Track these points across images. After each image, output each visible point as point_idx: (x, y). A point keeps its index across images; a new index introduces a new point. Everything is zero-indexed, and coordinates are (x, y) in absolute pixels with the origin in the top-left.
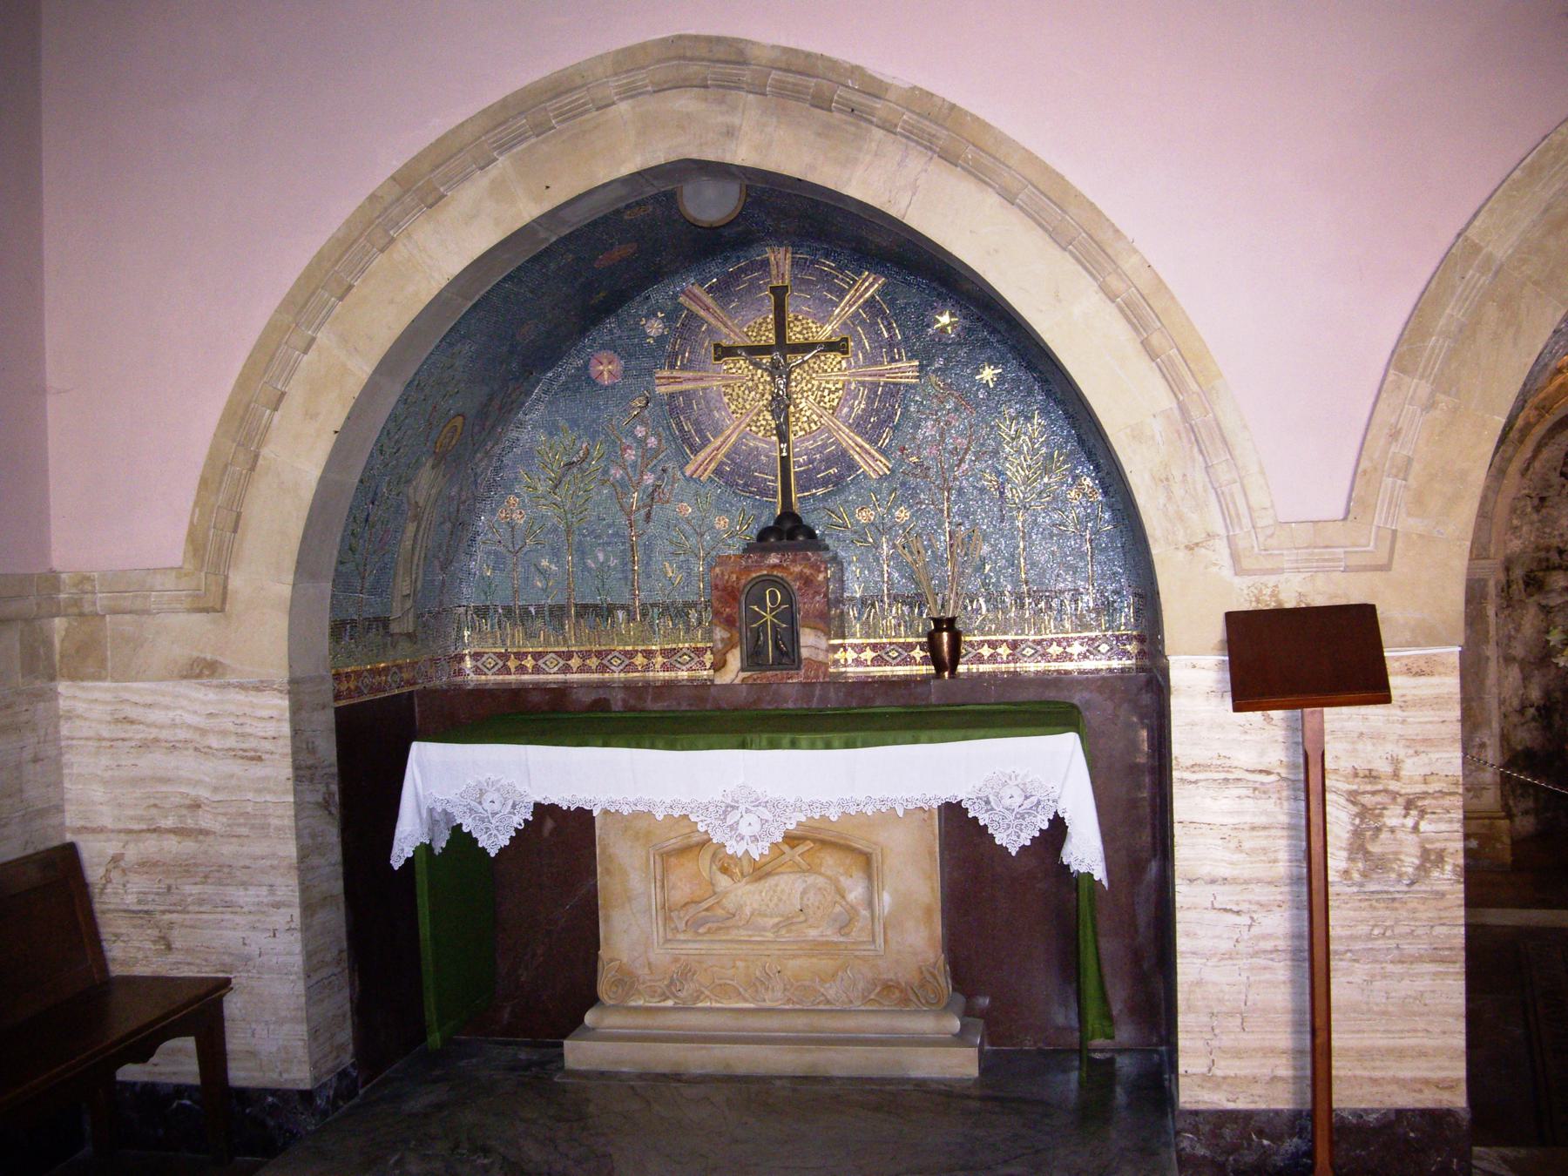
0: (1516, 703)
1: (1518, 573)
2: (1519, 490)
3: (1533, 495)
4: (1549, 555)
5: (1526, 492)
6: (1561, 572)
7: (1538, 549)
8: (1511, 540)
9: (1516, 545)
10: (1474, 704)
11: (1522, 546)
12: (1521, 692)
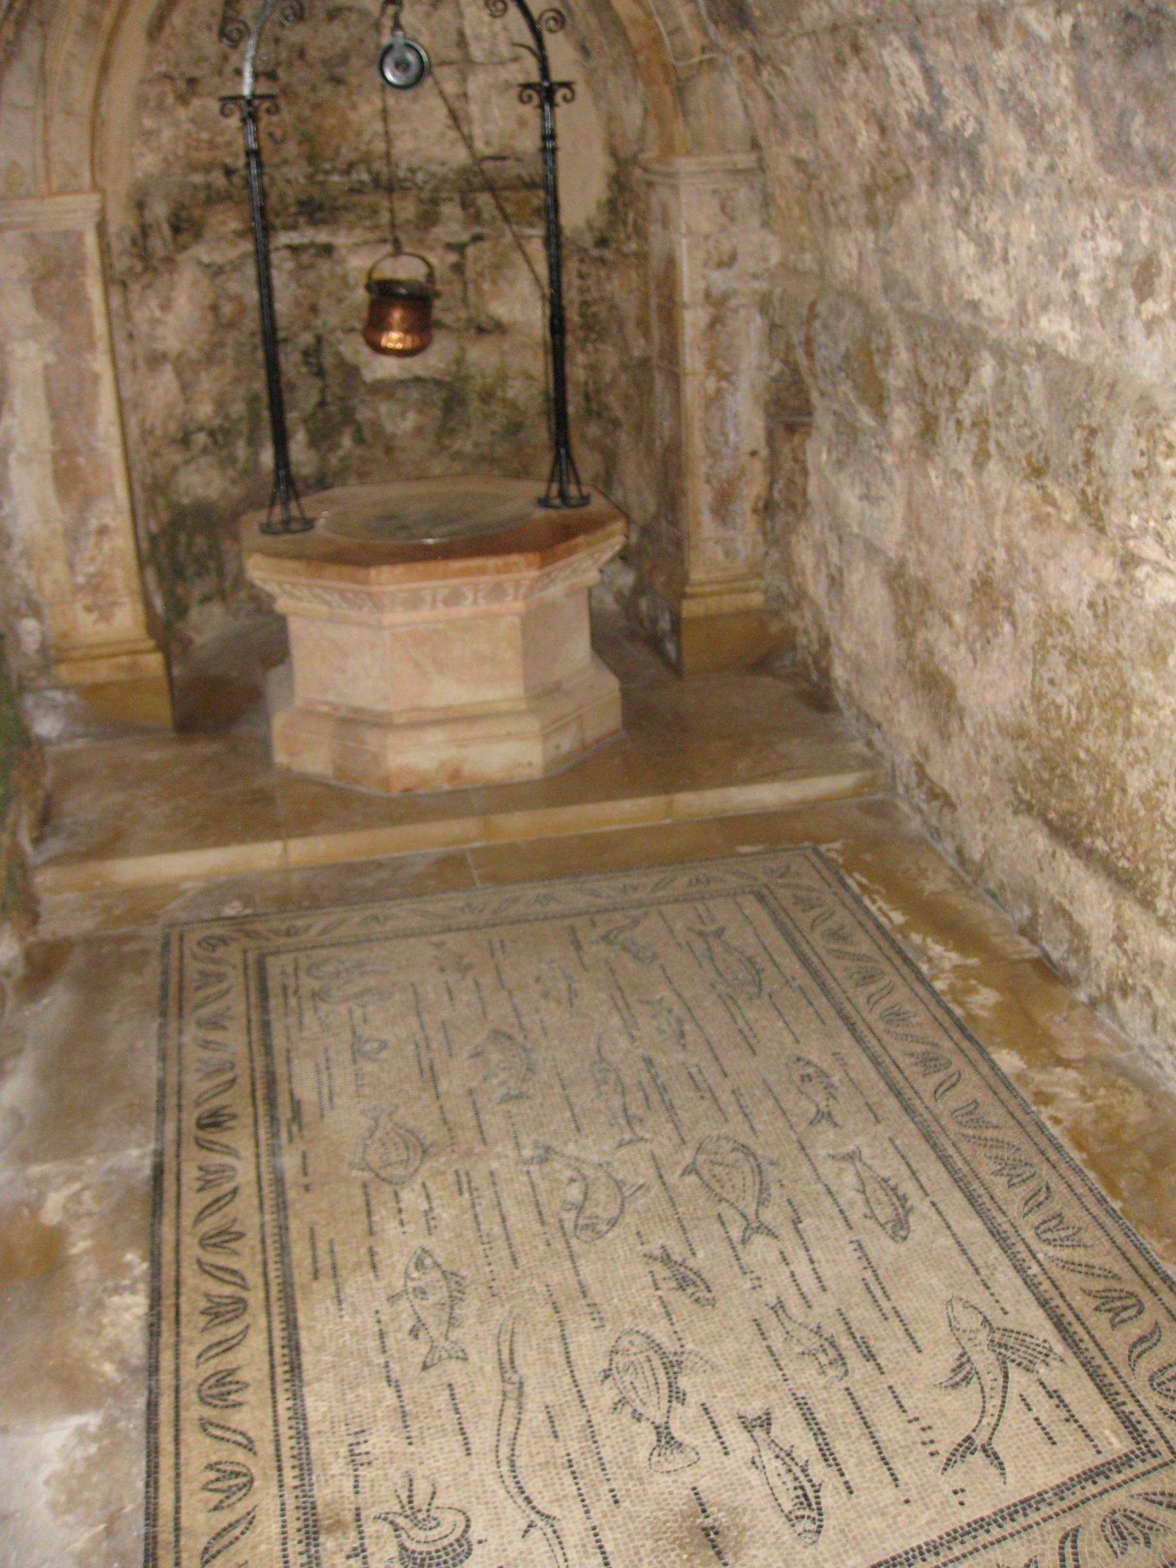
1: (159, 211)
3: (176, 74)
4: (210, 178)
5: (163, 68)
8: (142, 155)
9: (149, 162)
10: (81, 460)
12: (179, 410)
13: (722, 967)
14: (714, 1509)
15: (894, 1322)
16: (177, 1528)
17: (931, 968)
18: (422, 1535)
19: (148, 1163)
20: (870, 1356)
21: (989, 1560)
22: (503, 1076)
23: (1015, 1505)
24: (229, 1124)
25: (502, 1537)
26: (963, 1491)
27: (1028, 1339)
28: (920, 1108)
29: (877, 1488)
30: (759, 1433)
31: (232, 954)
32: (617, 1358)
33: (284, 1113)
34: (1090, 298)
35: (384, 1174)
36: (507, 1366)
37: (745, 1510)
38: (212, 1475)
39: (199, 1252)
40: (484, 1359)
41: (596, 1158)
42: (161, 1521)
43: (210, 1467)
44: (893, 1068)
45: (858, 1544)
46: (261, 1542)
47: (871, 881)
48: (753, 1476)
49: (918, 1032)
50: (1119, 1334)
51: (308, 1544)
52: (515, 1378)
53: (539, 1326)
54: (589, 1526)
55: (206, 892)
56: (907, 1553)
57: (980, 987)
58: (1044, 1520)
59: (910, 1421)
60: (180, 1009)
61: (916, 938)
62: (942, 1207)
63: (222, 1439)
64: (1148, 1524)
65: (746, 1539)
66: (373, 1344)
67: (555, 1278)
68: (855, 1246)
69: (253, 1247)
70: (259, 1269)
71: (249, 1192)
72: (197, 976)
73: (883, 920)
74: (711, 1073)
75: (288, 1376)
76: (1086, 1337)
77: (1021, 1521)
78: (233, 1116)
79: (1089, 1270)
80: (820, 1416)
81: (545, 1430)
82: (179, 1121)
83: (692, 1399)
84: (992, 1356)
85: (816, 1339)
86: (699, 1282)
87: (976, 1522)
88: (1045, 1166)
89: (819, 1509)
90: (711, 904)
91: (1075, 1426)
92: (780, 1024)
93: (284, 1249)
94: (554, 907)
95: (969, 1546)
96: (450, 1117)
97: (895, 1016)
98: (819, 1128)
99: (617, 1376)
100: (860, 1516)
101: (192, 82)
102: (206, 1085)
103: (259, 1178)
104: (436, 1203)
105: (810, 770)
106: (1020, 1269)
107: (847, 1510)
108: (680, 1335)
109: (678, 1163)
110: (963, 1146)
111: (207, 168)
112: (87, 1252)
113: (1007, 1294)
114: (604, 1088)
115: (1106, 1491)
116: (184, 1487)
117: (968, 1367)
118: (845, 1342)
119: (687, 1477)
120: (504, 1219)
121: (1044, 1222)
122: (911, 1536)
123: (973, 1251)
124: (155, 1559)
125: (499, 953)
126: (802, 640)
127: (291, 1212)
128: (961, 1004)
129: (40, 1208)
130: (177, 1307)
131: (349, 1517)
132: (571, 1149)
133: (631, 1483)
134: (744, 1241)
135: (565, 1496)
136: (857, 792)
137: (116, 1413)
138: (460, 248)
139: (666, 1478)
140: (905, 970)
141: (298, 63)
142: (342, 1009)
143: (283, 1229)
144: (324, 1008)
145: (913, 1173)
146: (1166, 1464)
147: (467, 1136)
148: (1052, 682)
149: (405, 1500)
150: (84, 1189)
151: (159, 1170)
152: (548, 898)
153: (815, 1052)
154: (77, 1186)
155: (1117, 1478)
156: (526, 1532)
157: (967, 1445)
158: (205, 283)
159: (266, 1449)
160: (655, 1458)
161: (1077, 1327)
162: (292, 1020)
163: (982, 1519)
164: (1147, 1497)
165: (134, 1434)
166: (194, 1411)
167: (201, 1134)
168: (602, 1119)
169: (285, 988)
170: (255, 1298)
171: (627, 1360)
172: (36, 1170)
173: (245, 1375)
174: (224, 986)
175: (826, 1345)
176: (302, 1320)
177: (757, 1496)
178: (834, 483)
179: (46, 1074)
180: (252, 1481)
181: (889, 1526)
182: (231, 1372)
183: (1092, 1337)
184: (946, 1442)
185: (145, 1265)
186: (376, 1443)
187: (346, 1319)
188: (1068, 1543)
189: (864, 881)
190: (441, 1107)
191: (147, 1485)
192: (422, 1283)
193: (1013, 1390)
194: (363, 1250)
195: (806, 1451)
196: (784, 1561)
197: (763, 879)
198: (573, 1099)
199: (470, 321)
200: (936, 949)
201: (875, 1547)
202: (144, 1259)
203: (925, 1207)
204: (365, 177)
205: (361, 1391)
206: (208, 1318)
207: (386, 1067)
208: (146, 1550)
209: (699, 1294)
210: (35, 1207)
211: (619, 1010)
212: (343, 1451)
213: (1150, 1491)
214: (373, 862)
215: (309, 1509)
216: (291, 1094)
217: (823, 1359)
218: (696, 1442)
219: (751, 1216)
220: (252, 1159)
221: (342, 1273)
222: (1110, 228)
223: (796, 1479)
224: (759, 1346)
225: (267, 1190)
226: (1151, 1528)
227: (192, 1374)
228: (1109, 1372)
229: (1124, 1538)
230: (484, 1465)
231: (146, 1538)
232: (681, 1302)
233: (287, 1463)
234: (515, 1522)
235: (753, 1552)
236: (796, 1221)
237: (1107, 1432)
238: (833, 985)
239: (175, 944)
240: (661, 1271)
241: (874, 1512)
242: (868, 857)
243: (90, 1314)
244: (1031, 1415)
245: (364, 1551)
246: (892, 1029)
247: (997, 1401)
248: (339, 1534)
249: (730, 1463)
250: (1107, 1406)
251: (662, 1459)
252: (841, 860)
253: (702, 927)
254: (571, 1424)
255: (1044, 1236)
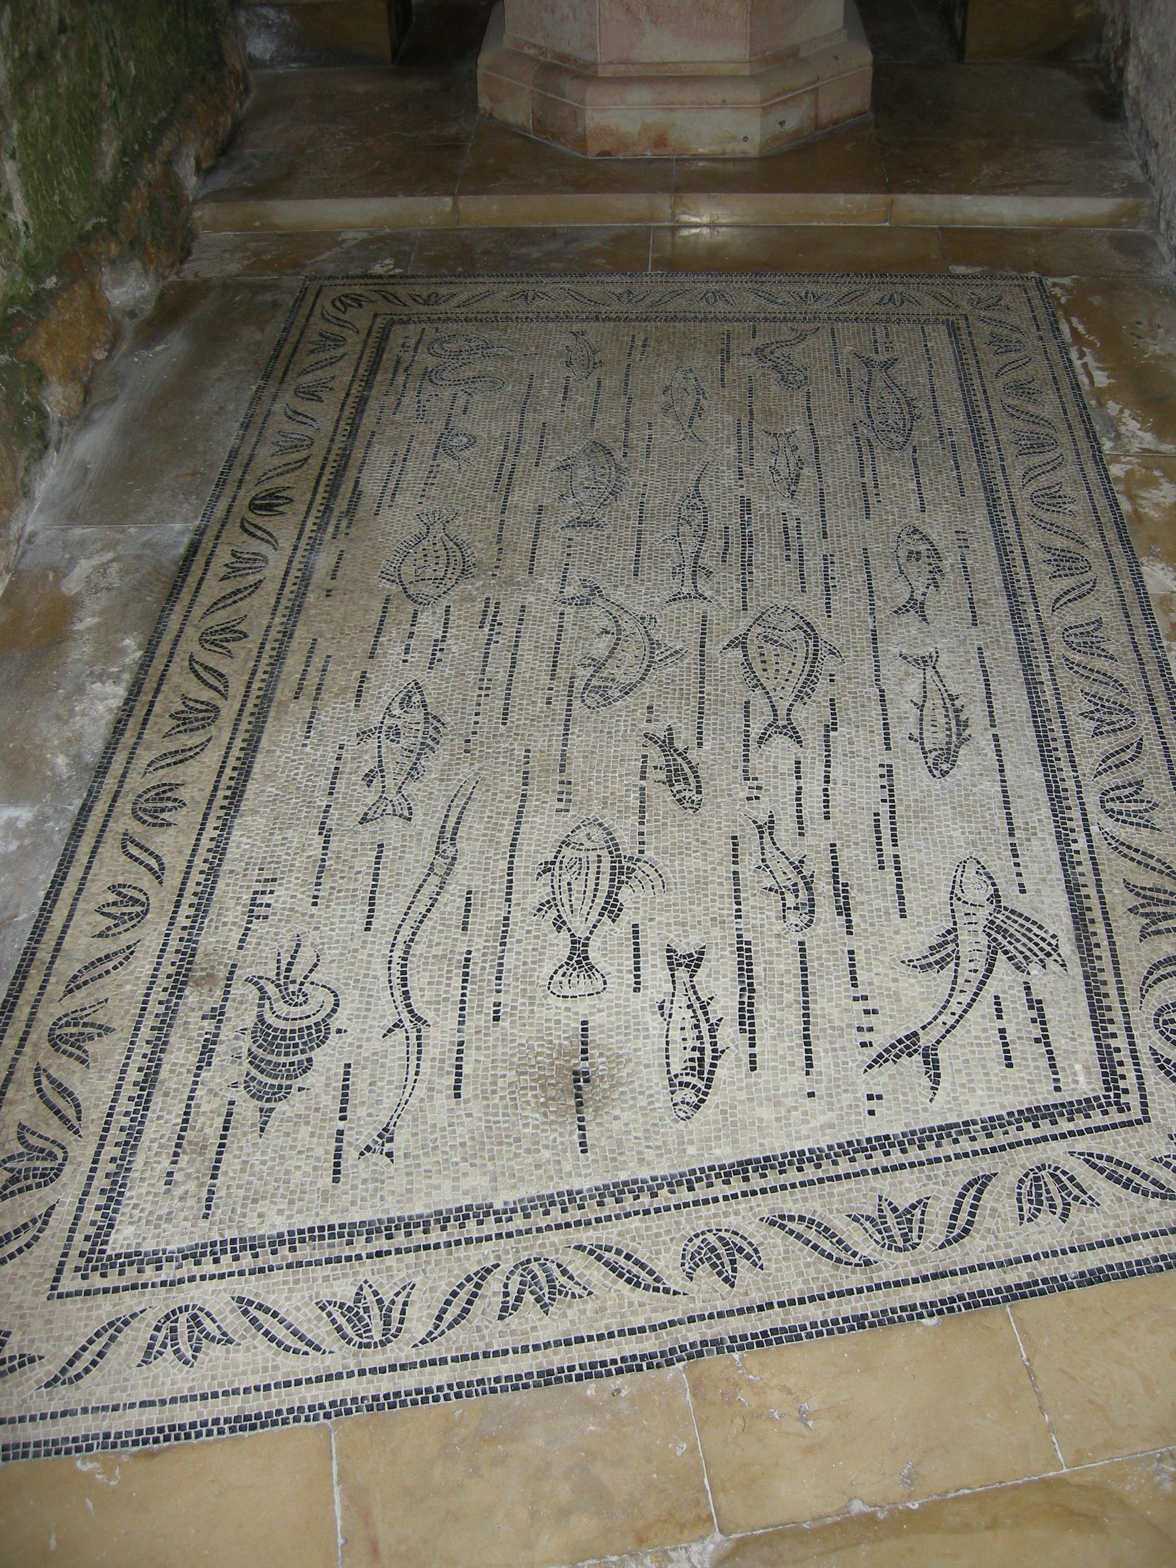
13: (874, 404)
14: (596, 1052)
15: (890, 872)
16: (57, 949)
17: (1114, 448)
18: (283, 1008)
19: (186, 540)
20: (844, 910)
21: (873, 1189)
22: (582, 495)
23: (932, 1130)
24: (280, 509)
25: (363, 1031)
26: (879, 1097)
27: (1035, 929)
28: (1031, 616)
29: (784, 1071)
30: (682, 974)
31: (361, 318)
32: (566, 851)
33: (341, 504)
35: (412, 590)
36: (447, 836)
37: (629, 1061)
38: (112, 897)
39: (196, 647)
40: (426, 825)
41: (640, 610)
42: (45, 938)
43: (112, 889)
44: (1019, 561)
45: (735, 1132)
46: (128, 981)
47: (1088, 331)
48: (654, 1022)
49: (1066, 522)
50: (1145, 947)
51: (171, 994)
52: (450, 852)
53: (500, 797)
54: (456, 1040)
55: (363, 244)
56: (784, 1156)
57: (1162, 480)
58: (957, 1156)
59: (856, 999)
60: (285, 373)
61: (1113, 408)
62: (1003, 743)
63: (137, 859)
64: (1076, 1192)
65: (615, 1096)
66: (323, 783)
67: (539, 743)
68: (884, 771)
69: (250, 650)
70: (246, 677)
71: (271, 587)
72: (316, 338)
73: (1083, 379)
74: (811, 529)
75: (226, 803)
76: (1105, 943)
77: (931, 1150)
78: (290, 500)
79: (1144, 859)
80: (757, 970)
81: (457, 919)
82: (234, 498)
83: (626, 918)
84: (984, 940)
85: (792, 874)
86: (692, 780)
87: (878, 1138)
88: (1148, 718)
89: (710, 1080)
90: (894, 328)
91: (1044, 1049)
92: (913, 485)
93: (279, 658)
94: (721, 307)
95: (857, 1167)
96: (506, 534)
97: (1050, 499)
98: (904, 619)
99: (557, 872)
100: (750, 1100)
102: (276, 462)
103: (287, 573)
104: (452, 631)
105: (1064, 188)
106: (1063, 839)
107: (740, 1089)
108: (645, 838)
109: (725, 632)
110: (1062, 673)
112: (89, 629)
113: (1035, 867)
114: (685, 529)
115: (1045, 1139)
116: (81, 905)
117: (950, 948)
118: (823, 886)
119: (582, 1008)
120: (514, 664)
121: (1118, 788)
122: (797, 1139)
123: (1016, 806)
124: (24, 978)
125: (637, 355)
126: (1109, 31)
127: (302, 617)
128: (1132, 498)
129: (65, 575)
130: (152, 704)
131: (223, 972)
132: (619, 596)
133: (521, 1001)
134: (761, 740)
135: (446, 1000)
136: (1113, 220)
137: (49, 811)
139: (561, 1003)
140: (1084, 445)
142: (447, 394)
143: (288, 634)
144: (429, 388)
145: (989, 694)
146: (1130, 1123)
147: (516, 560)
149: (283, 967)
150: (113, 560)
151: (193, 549)
152: (718, 295)
153: (938, 528)
154: (110, 555)
155: (1065, 1126)
156: (390, 1031)
157: (908, 1044)
159: (173, 880)
160: (557, 978)
161: (1100, 928)
162: (392, 399)
163: (887, 1137)
164: (1089, 1159)
165: (56, 838)
166: (124, 823)
167: (250, 516)
168: (668, 565)
169: (398, 362)
170: (229, 710)
171: (577, 854)
172: (78, 532)
173: (184, 794)
174: (340, 351)
175: (801, 884)
176: (264, 743)
177: (649, 1049)
179: (125, 431)
180: (146, 912)
181: (778, 1120)
182: (173, 787)
183: (1112, 943)
184: (885, 1034)
185: (139, 654)
186: (281, 897)
187: (308, 749)
188: (972, 1192)
189: (1081, 329)
190: (502, 522)
191: (47, 897)
192: (399, 723)
193: (992, 987)
194: (357, 674)
195: (724, 1008)
196: (647, 1131)
197: (967, 308)
198: (646, 536)
200: (1131, 425)
201: (753, 1140)
202: (140, 648)
203: (984, 740)
205: (290, 834)
206: (175, 722)
207: (464, 467)
208: (20, 966)
209: (687, 794)
210: (61, 573)
211: (740, 438)
212: (246, 897)
213: (1095, 1152)
214: (543, 231)
215: (188, 955)
216: (357, 483)
217: (791, 901)
218: (609, 969)
219: (782, 712)
220: (289, 552)
221: (325, 695)
223: (700, 1038)
224: (727, 868)
225: (289, 587)
226: (1076, 1198)
227: (136, 782)
228: (1113, 992)
229: (1040, 1203)
230: (379, 942)
231: (25, 954)
232: (662, 798)
233: (188, 898)
234: (383, 1017)
235: (617, 1112)
236: (832, 727)
237: (1078, 1067)
238: (993, 448)
239: (310, 298)
240: (656, 756)
241: (769, 1100)
242: (1097, 300)
243: (68, 698)
244: (999, 1024)
245: (222, 1014)
246: (1040, 514)
247: (966, 999)
248: (205, 991)
249: (636, 1001)
250: (1092, 1035)
251: (565, 980)
252: (1063, 300)
253: (873, 355)
254: (486, 919)
255: (1109, 805)
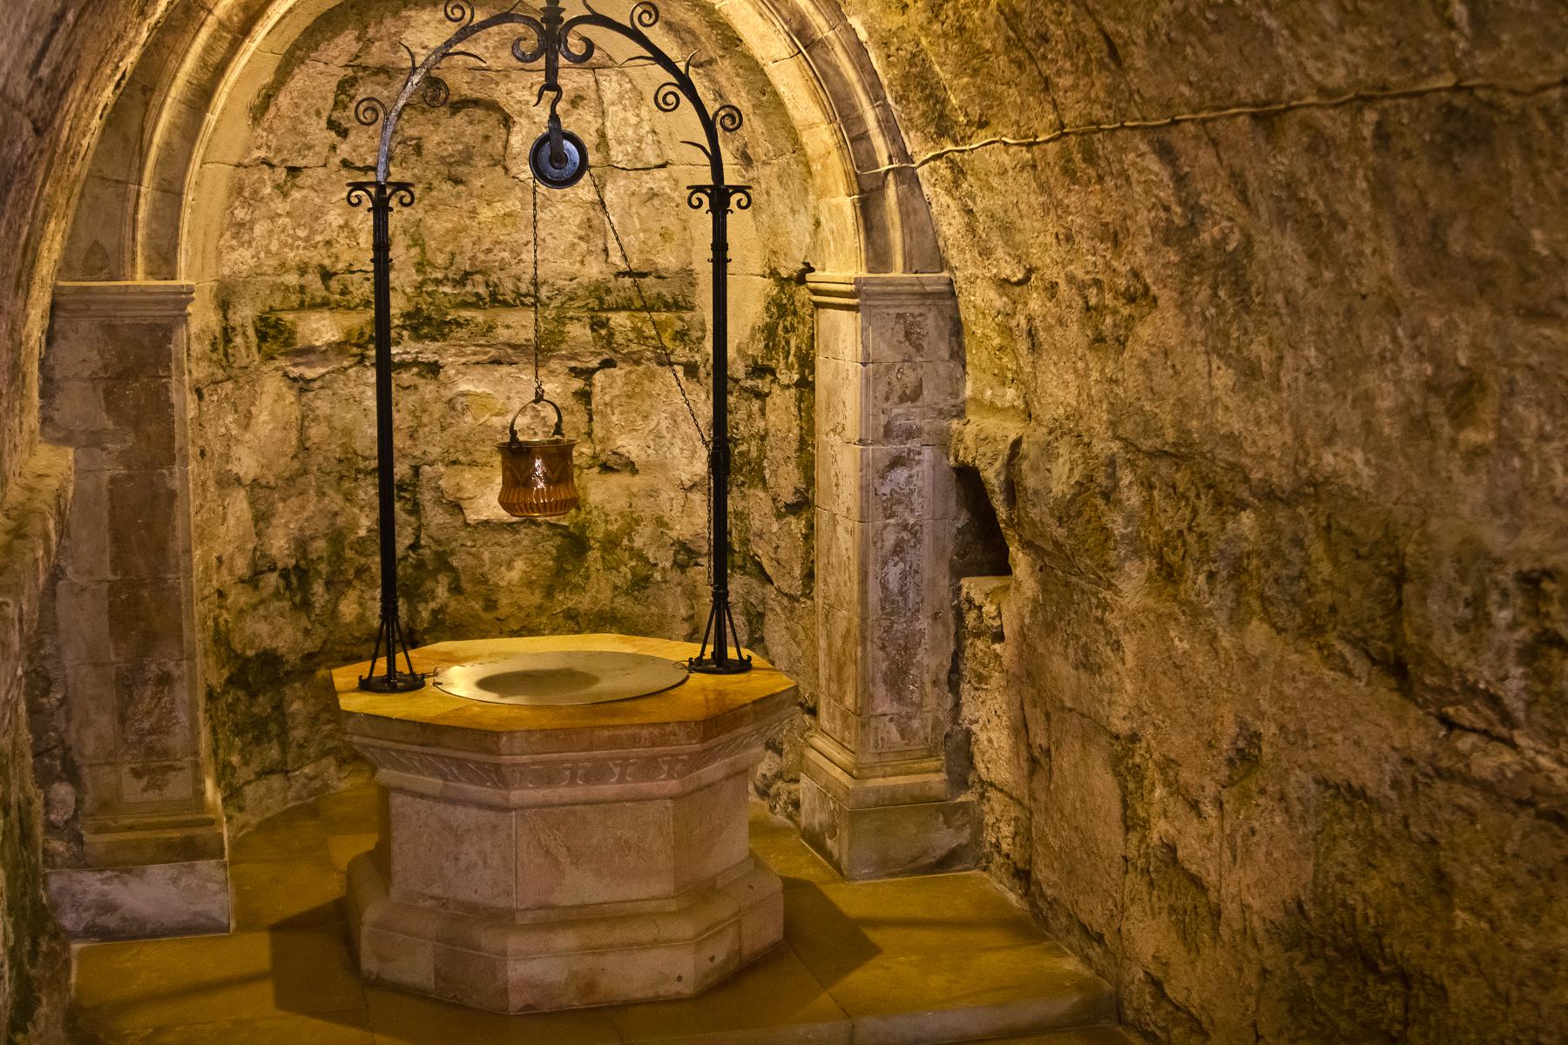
0: (242, 565)
1: (245, 314)
2: (248, 151)
3: (275, 161)
5: (262, 154)
6: (327, 314)
7: (283, 267)
8: (233, 249)
10: (145, 593)
11: (252, 262)
34: (1390, 429)
101: (294, 171)
111: (303, 270)
138: (587, 374)
141: (413, 158)
148: (1341, 878)
158: (291, 397)
178: (1040, 650)
199: (595, 457)
204: (482, 290)
222: (1417, 348)
